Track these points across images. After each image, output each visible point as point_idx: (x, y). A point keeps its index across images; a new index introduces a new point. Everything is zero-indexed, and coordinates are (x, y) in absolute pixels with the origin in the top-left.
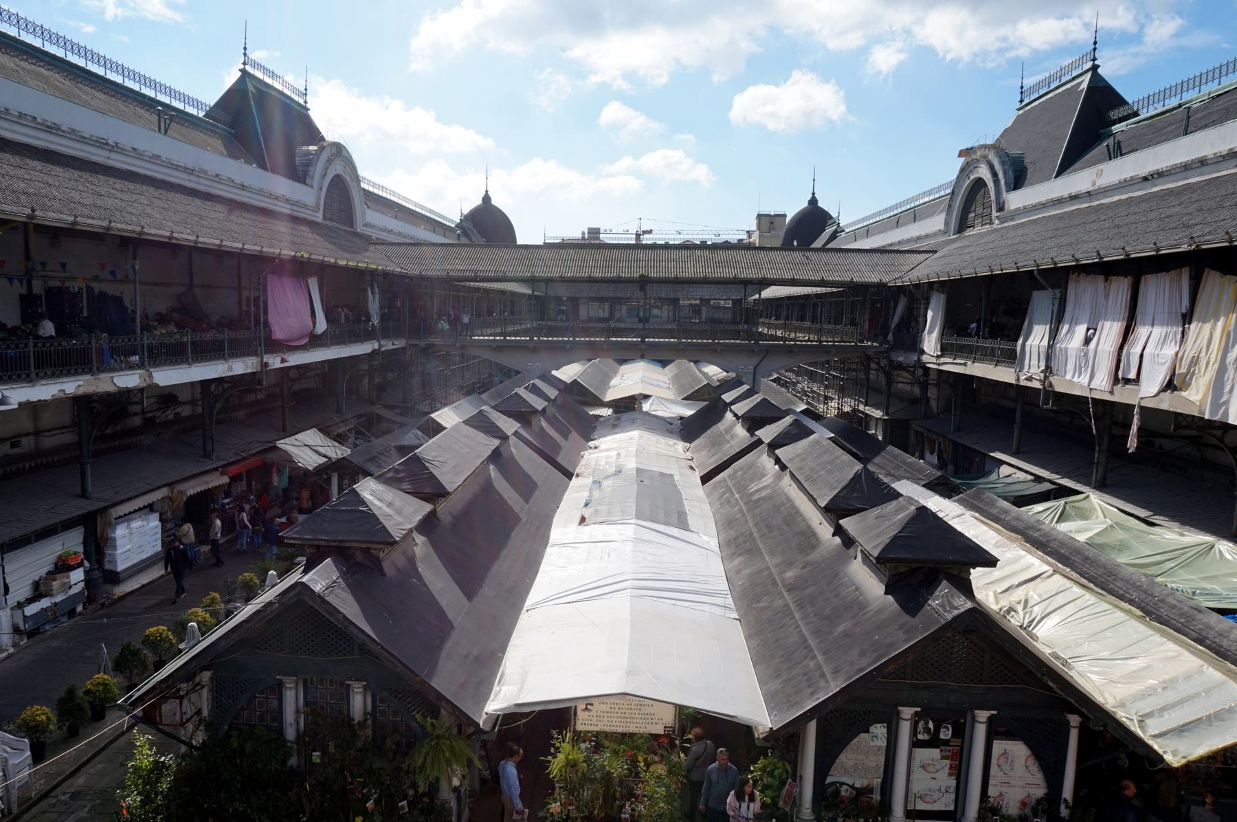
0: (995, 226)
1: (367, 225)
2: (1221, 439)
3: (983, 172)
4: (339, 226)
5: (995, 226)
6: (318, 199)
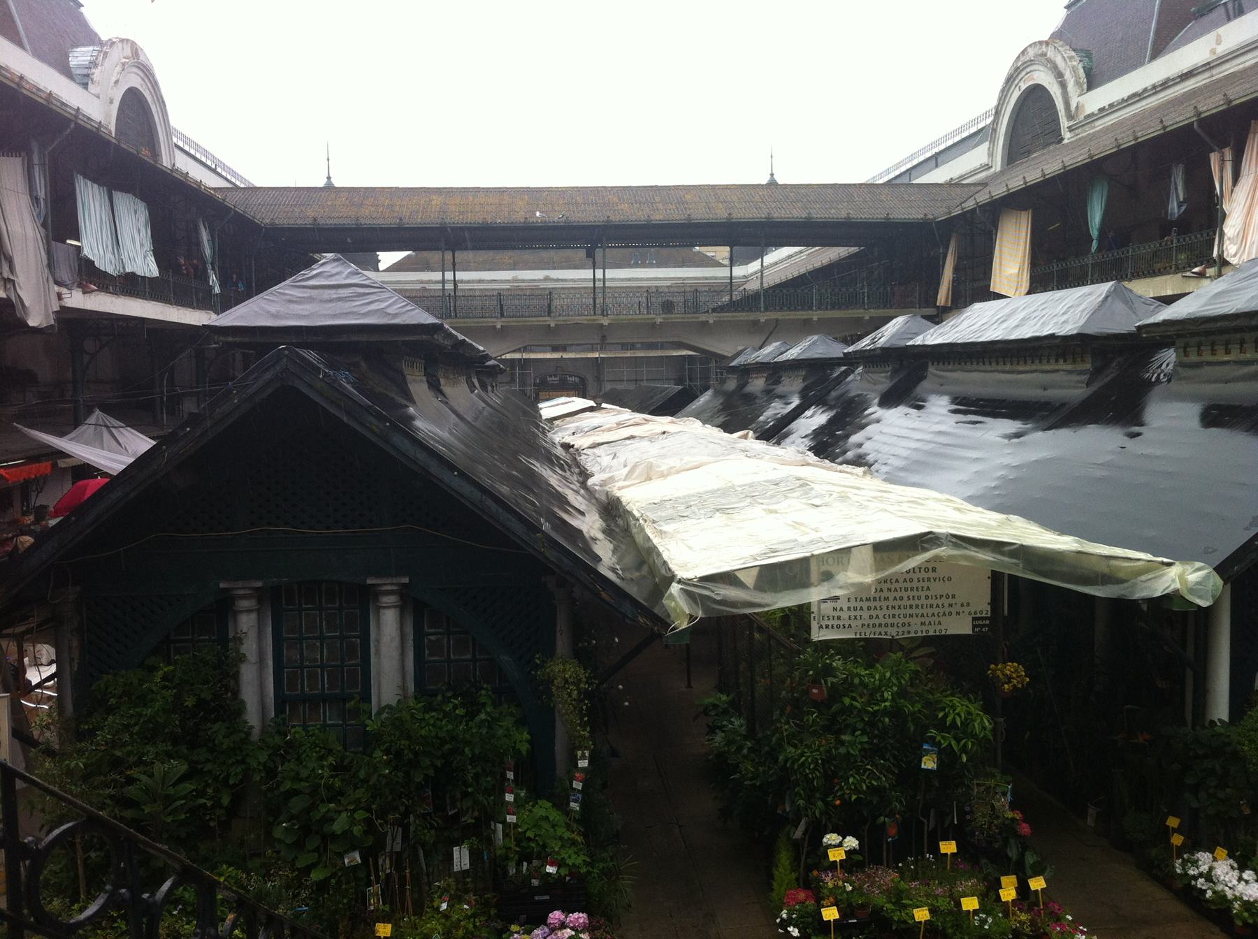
0: (1066, 141)
6: (108, 115)
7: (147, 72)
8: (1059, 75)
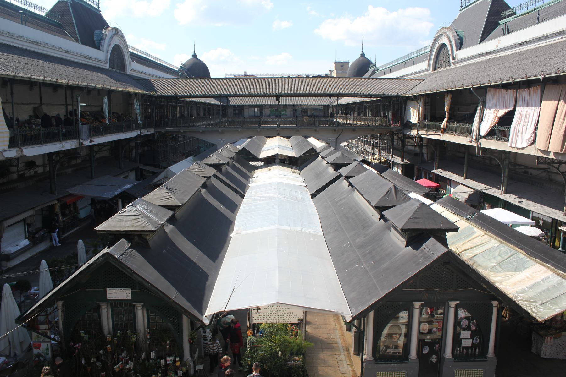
0: (452, 67)
1: (131, 70)
2: (558, 169)
3: (445, 40)
4: (118, 71)
5: (452, 67)
6: (107, 57)
7: (122, 37)
8: (450, 42)
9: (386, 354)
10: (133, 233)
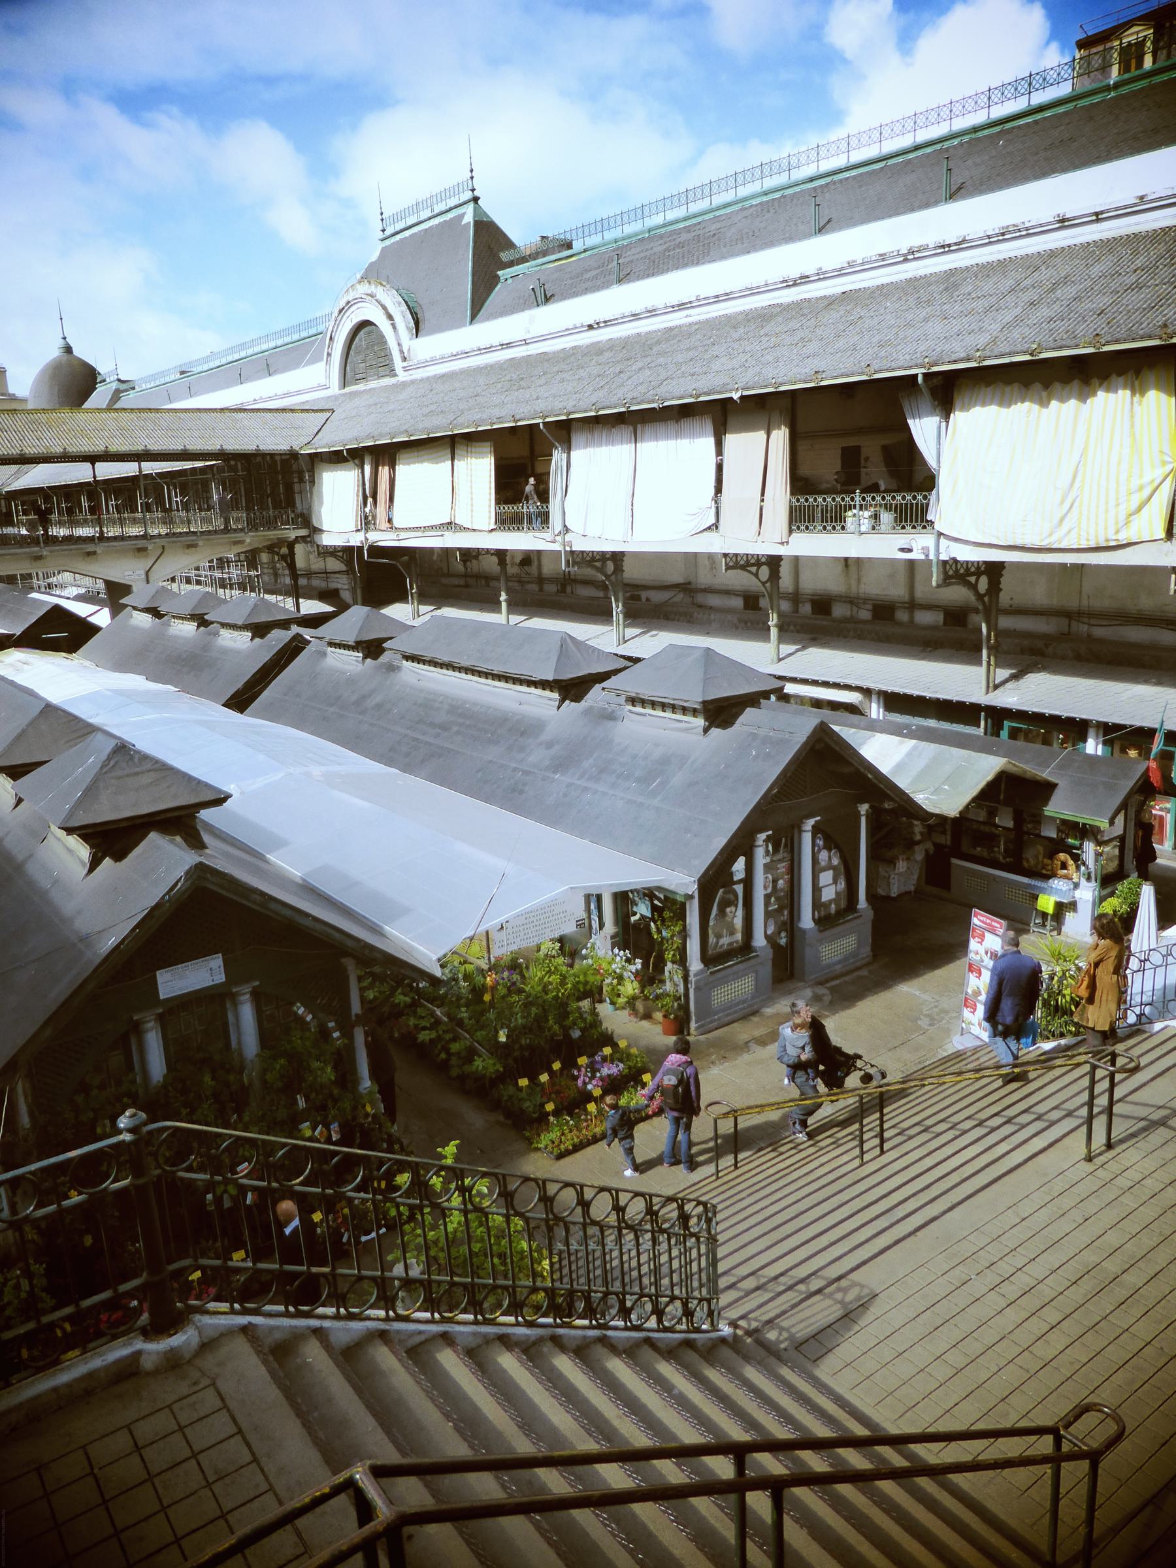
2: (756, 575)
9: (718, 950)
10: (169, 815)
